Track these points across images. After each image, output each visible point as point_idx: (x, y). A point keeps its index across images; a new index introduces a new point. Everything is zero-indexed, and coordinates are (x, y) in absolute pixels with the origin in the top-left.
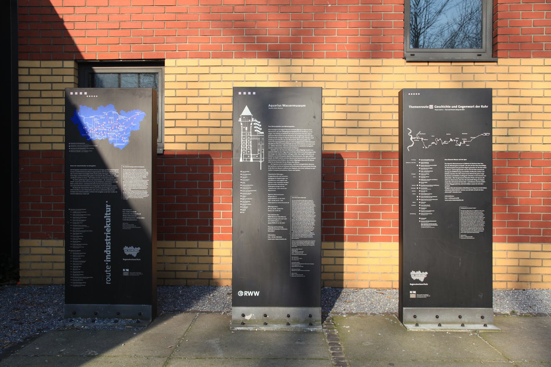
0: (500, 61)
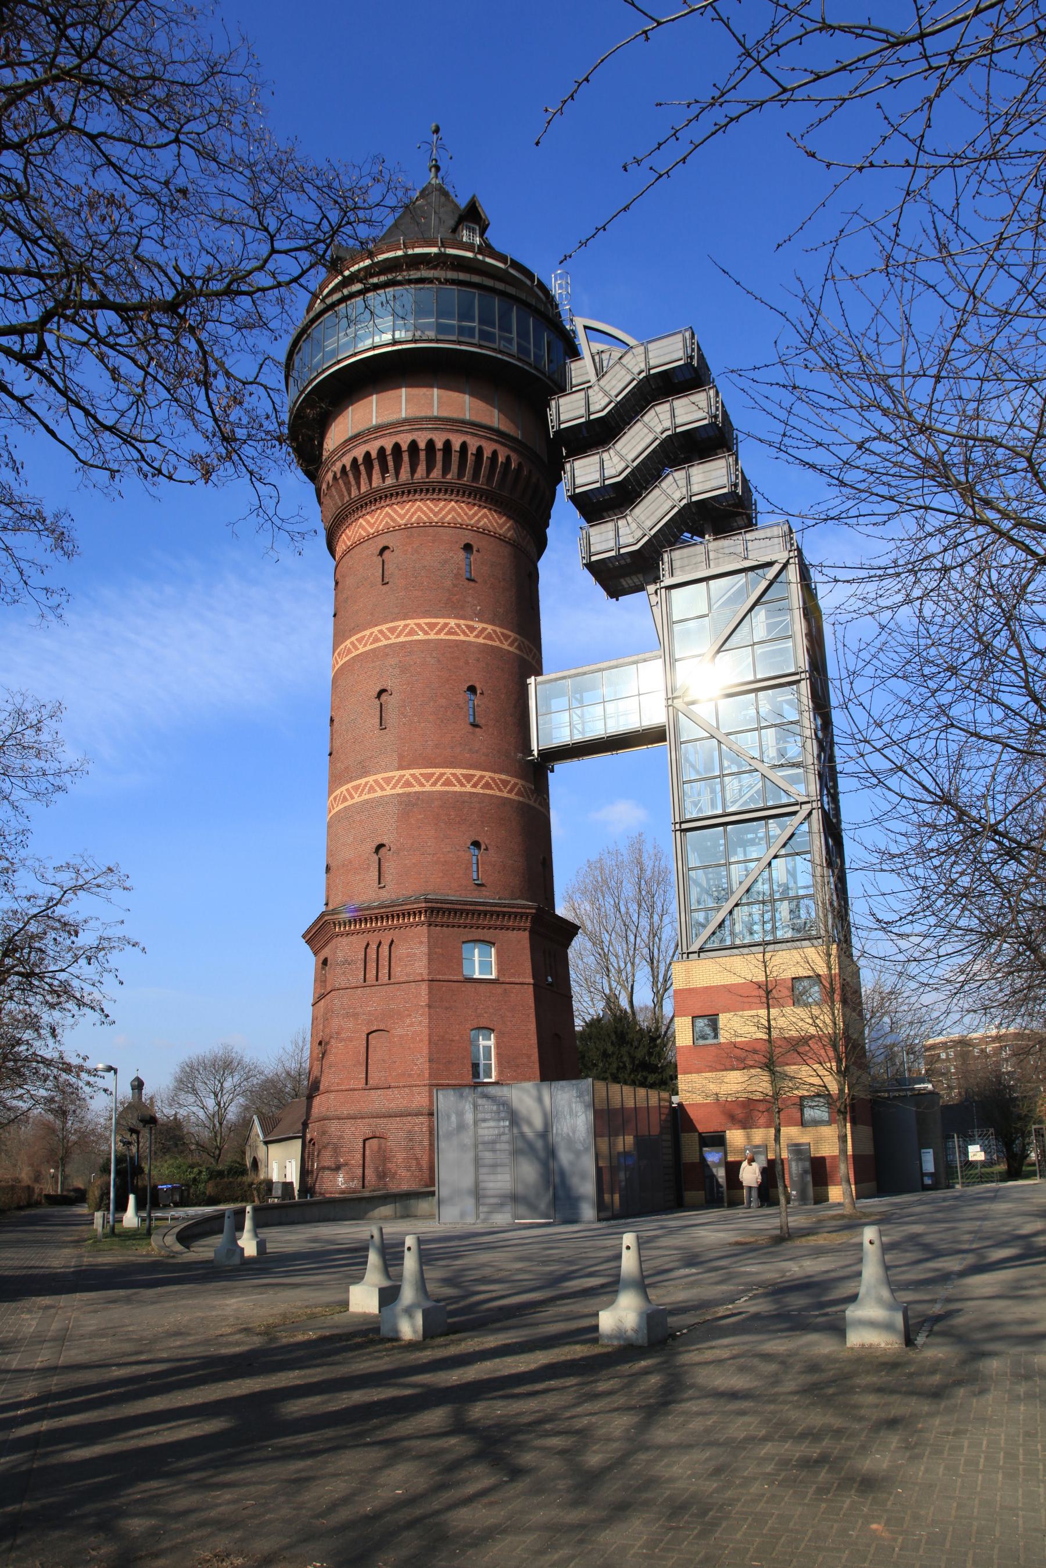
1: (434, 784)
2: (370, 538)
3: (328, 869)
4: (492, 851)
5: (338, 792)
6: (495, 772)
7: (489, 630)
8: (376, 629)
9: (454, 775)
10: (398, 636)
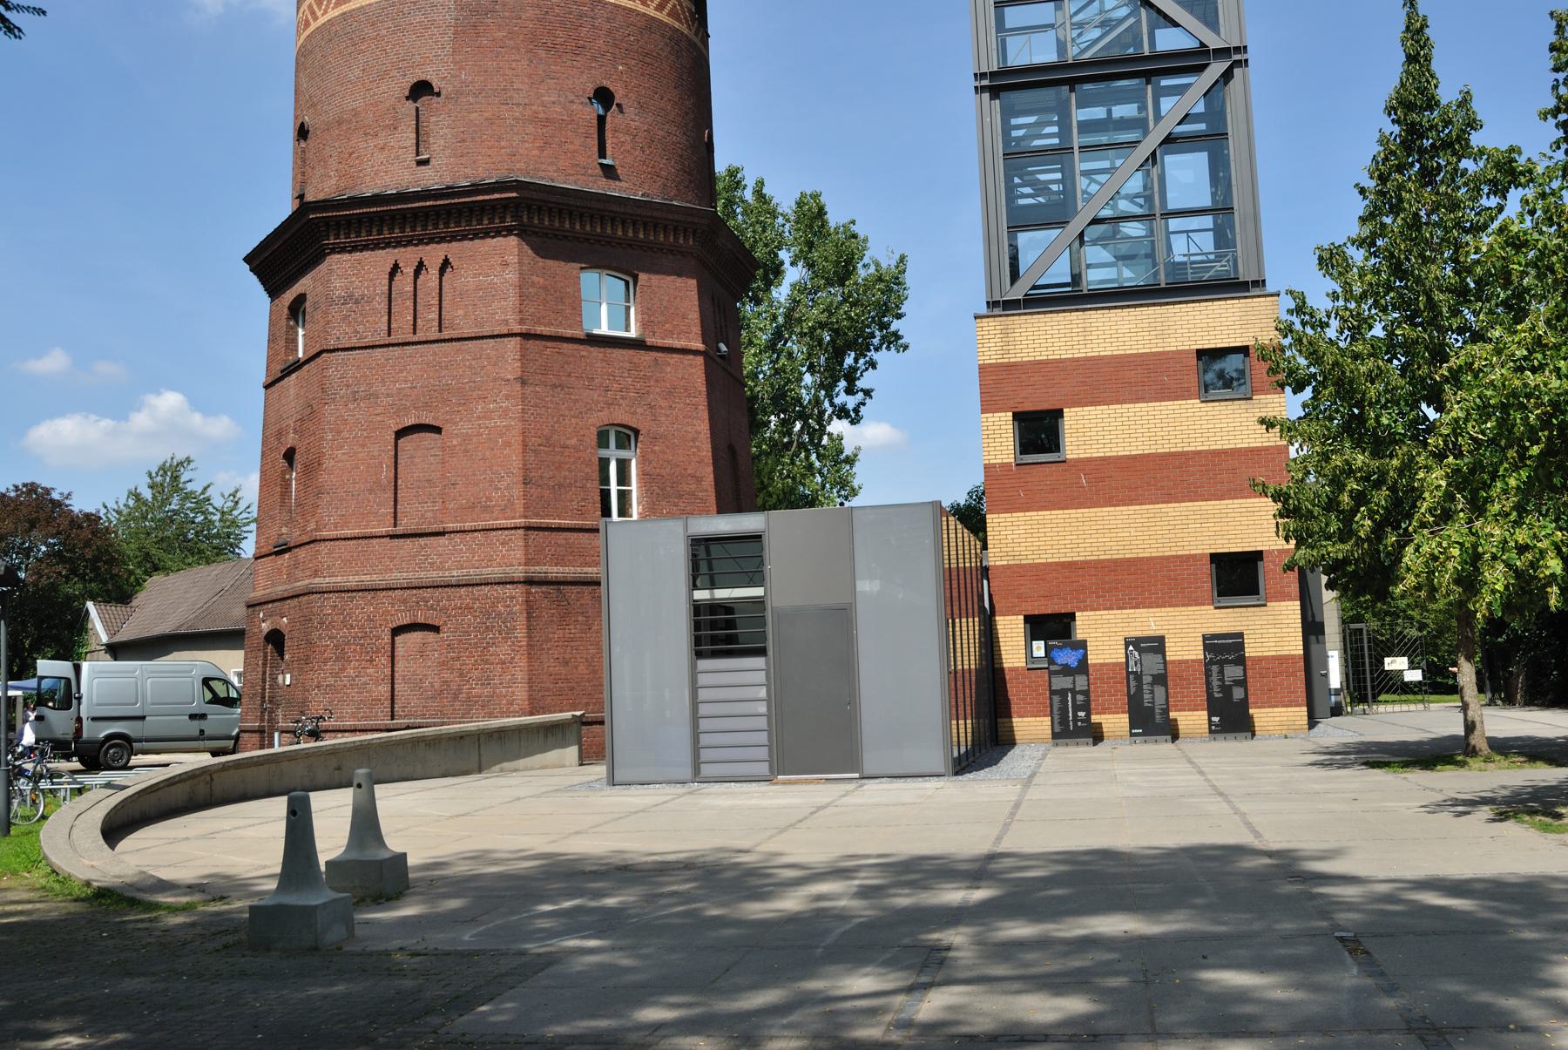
0: (1268, 604)
3: (303, 133)
4: (630, 111)
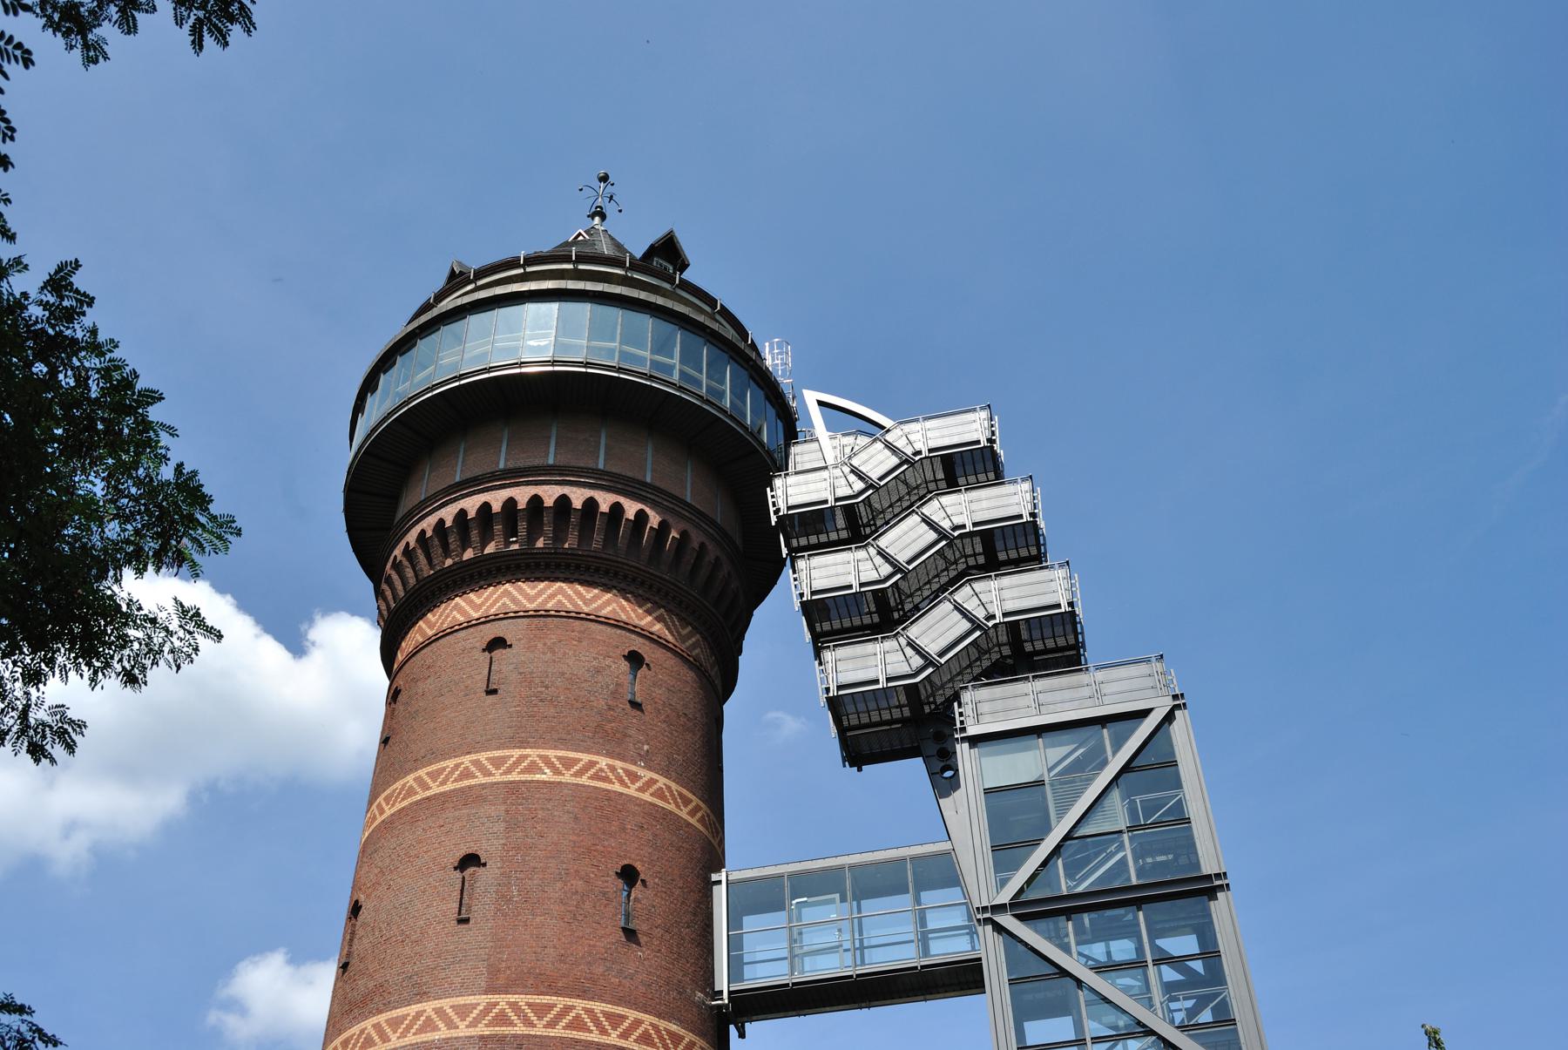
1: (552, 1024)
2: (470, 625)
5: (355, 1030)
6: (659, 1016)
7: (660, 784)
8: (466, 760)
9: (589, 1011)
10: (508, 771)
